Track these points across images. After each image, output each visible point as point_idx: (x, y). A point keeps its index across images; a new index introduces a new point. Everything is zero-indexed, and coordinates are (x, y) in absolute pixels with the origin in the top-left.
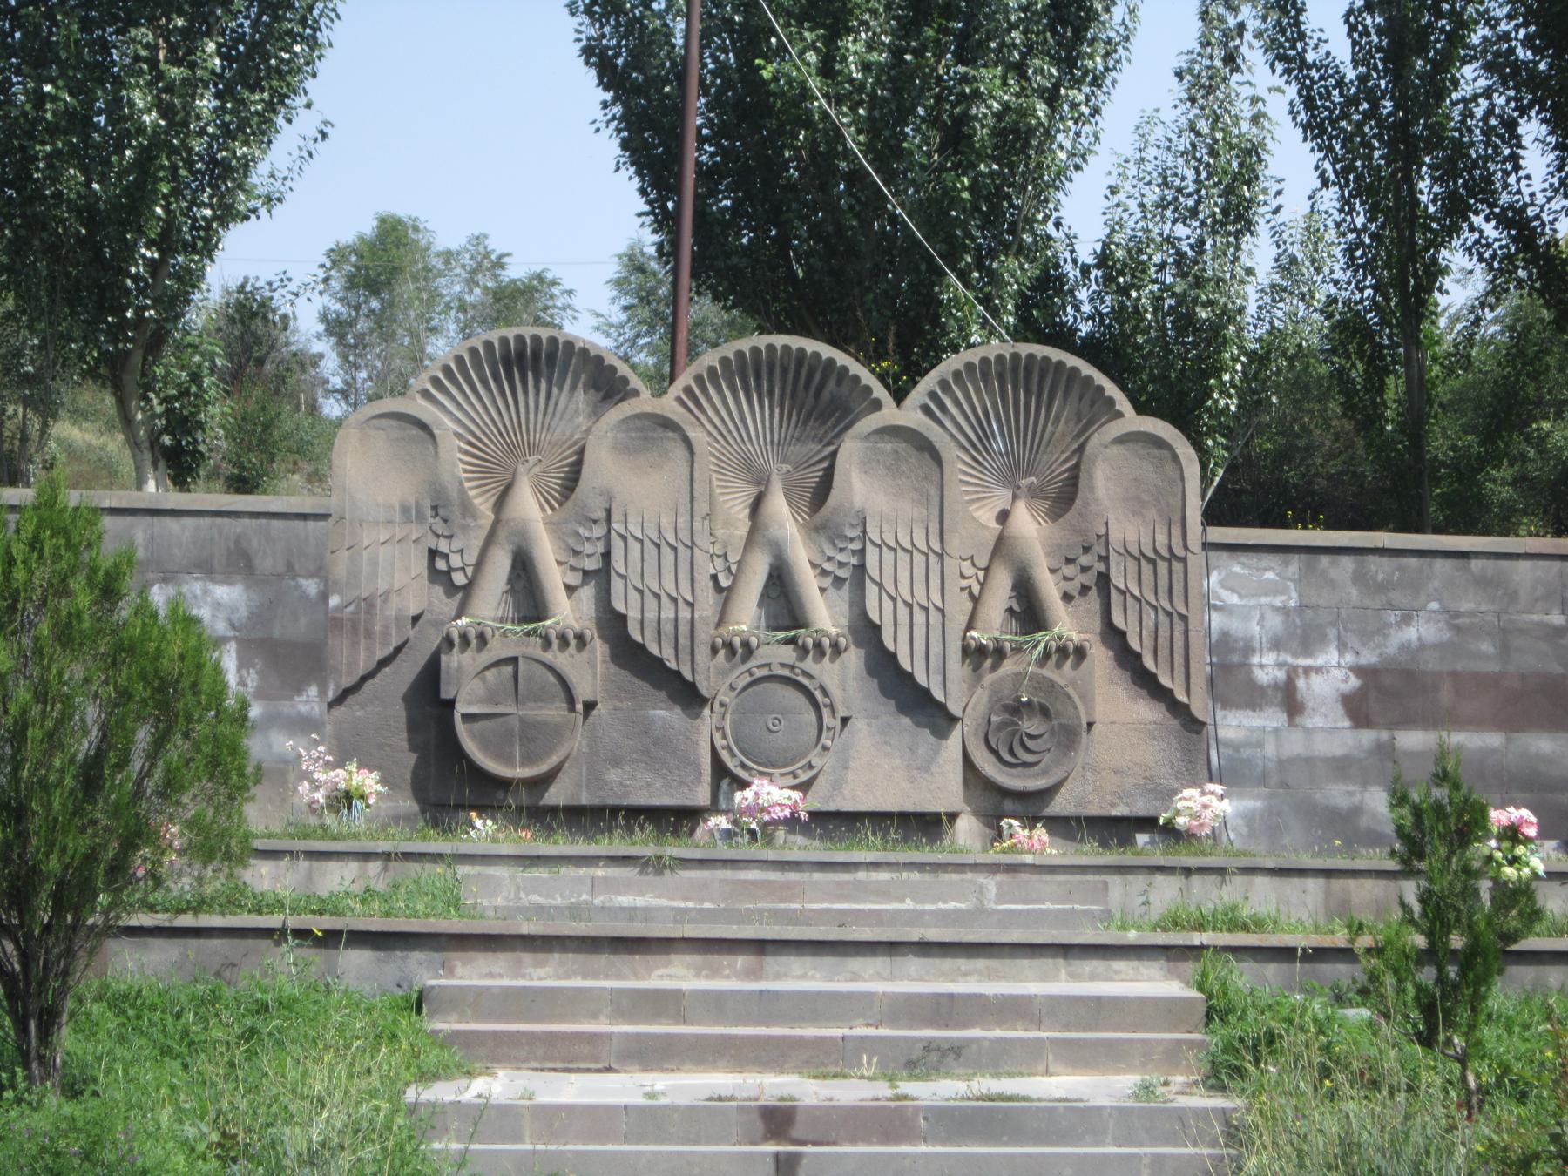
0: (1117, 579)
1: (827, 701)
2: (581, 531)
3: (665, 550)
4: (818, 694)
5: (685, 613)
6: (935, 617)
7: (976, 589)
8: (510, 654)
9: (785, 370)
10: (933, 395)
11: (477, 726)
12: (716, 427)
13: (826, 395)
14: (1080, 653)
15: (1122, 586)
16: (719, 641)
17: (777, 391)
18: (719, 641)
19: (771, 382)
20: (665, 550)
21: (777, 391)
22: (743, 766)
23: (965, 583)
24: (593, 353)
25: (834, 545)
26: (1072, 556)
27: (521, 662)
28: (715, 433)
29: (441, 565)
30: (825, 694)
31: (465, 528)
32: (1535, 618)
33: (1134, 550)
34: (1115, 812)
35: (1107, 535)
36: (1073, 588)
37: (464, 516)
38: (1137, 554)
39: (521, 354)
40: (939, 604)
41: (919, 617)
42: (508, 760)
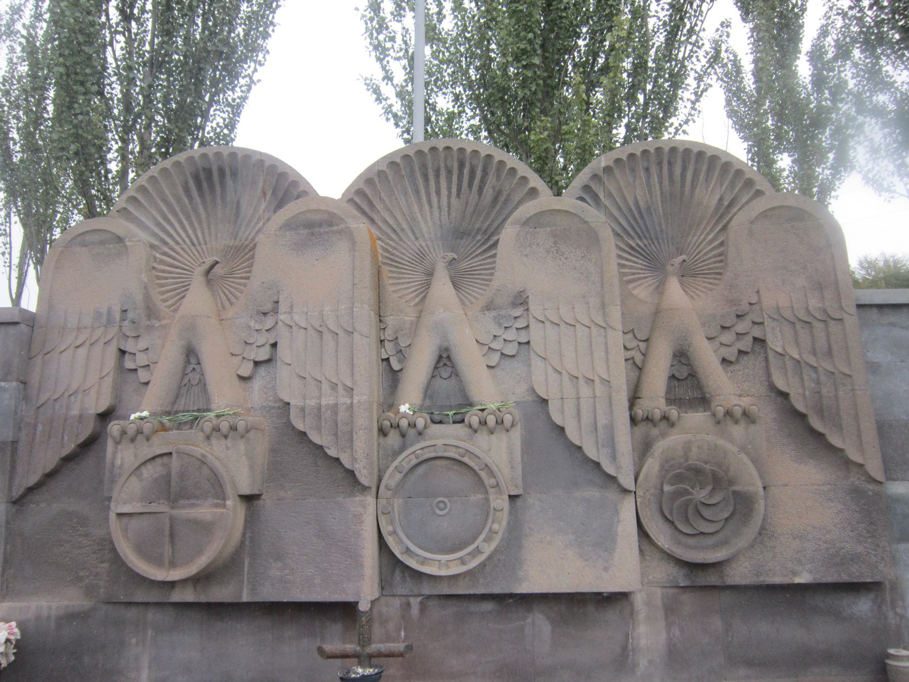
0: (775, 343)
1: (493, 481)
2: (252, 324)
3: (327, 336)
4: (483, 474)
5: (344, 400)
6: (600, 389)
7: (638, 358)
8: (165, 451)
9: (449, 172)
10: (586, 188)
11: (134, 523)
12: (389, 225)
13: (489, 192)
14: (748, 416)
15: (779, 350)
16: (387, 423)
17: (444, 192)
18: (387, 423)
19: (438, 183)
20: (327, 336)
21: (444, 192)
22: (408, 551)
23: (629, 354)
24: (267, 164)
25: (500, 325)
26: (727, 325)
27: (174, 455)
28: (389, 231)
29: (129, 364)
30: (492, 474)
31: (150, 328)
33: (787, 314)
34: (797, 580)
35: (759, 302)
36: (731, 353)
37: (149, 317)
38: (792, 319)
39: (208, 172)
40: (605, 376)
41: (585, 391)
42: (157, 561)
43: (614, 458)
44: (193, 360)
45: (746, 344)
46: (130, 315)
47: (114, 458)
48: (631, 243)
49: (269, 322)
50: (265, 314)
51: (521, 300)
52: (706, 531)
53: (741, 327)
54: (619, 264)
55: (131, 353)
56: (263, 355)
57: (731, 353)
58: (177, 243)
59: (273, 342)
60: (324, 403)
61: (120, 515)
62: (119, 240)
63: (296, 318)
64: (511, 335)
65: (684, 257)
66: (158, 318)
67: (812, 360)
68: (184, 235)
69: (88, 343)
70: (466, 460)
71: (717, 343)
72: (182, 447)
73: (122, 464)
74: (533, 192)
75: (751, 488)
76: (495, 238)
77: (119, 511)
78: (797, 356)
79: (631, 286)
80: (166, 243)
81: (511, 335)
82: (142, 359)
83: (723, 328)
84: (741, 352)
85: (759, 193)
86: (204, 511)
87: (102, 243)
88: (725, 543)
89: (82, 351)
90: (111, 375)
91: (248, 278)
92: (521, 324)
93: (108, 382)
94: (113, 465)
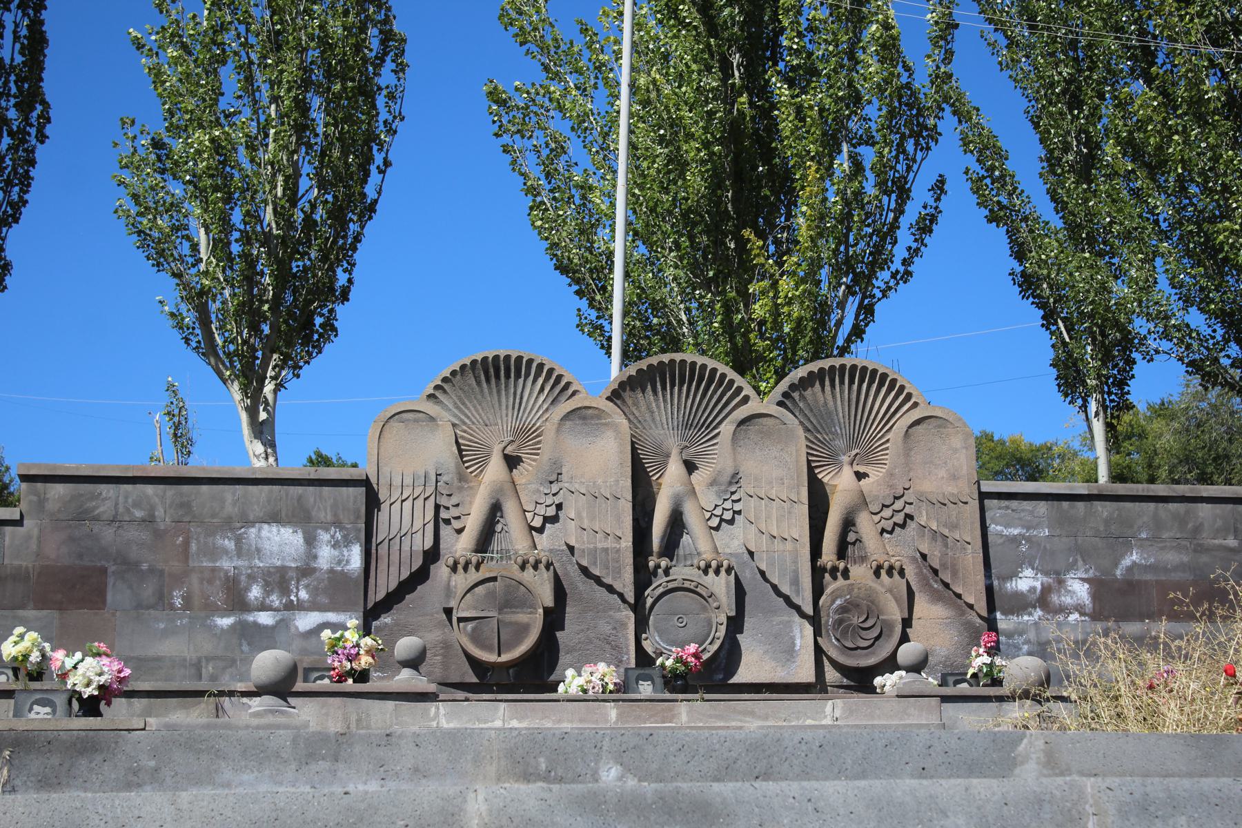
2: (541, 489)
10: (786, 395)
15: (923, 523)
20: (601, 500)
25: (720, 497)
27: (499, 579)
31: (460, 489)
32: (1216, 541)
43: (798, 592)
44: (499, 514)
45: (899, 518)
46: (444, 478)
47: (449, 581)
48: (819, 436)
49: (555, 488)
50: (551, 483)
51: (735, 479)
52: (861, 645)
53: (898, 505)
54: (808, 453)
55: (445, 507)
56: (551, 512)
57: (888, 525)
58: (473, 423)
59: (557, 502)
60: (599, 545)
61: (460, 620)
62: (432, 419)
63: (577, 486)
64: (728, 505)
65: (857, 451)
66: (466, 481)
67: (946, 532)
68: (478, 417)
69: (411, 498)
70: (698, 590)
71: (879, 515)
72: (505, 573)
73: (456, 587)
74: (746, 399)
75: (894, 617)
76: (717, 431)
77: (459, 615)
78: (935, 528)
79: (817, 471)
80: (465, 423)
81: (728, 505)
82: (454, 512)
83: (884, 506)
84: (895, 524)
85: (916, 405)
86: (522, 617)
87: (416, 421)
88: (873, 653)
89: (408, 504)
90: (432, 521)
91: (537, 454)
92: (735, 497)
93: (430, 528)
94: (449, 584)
